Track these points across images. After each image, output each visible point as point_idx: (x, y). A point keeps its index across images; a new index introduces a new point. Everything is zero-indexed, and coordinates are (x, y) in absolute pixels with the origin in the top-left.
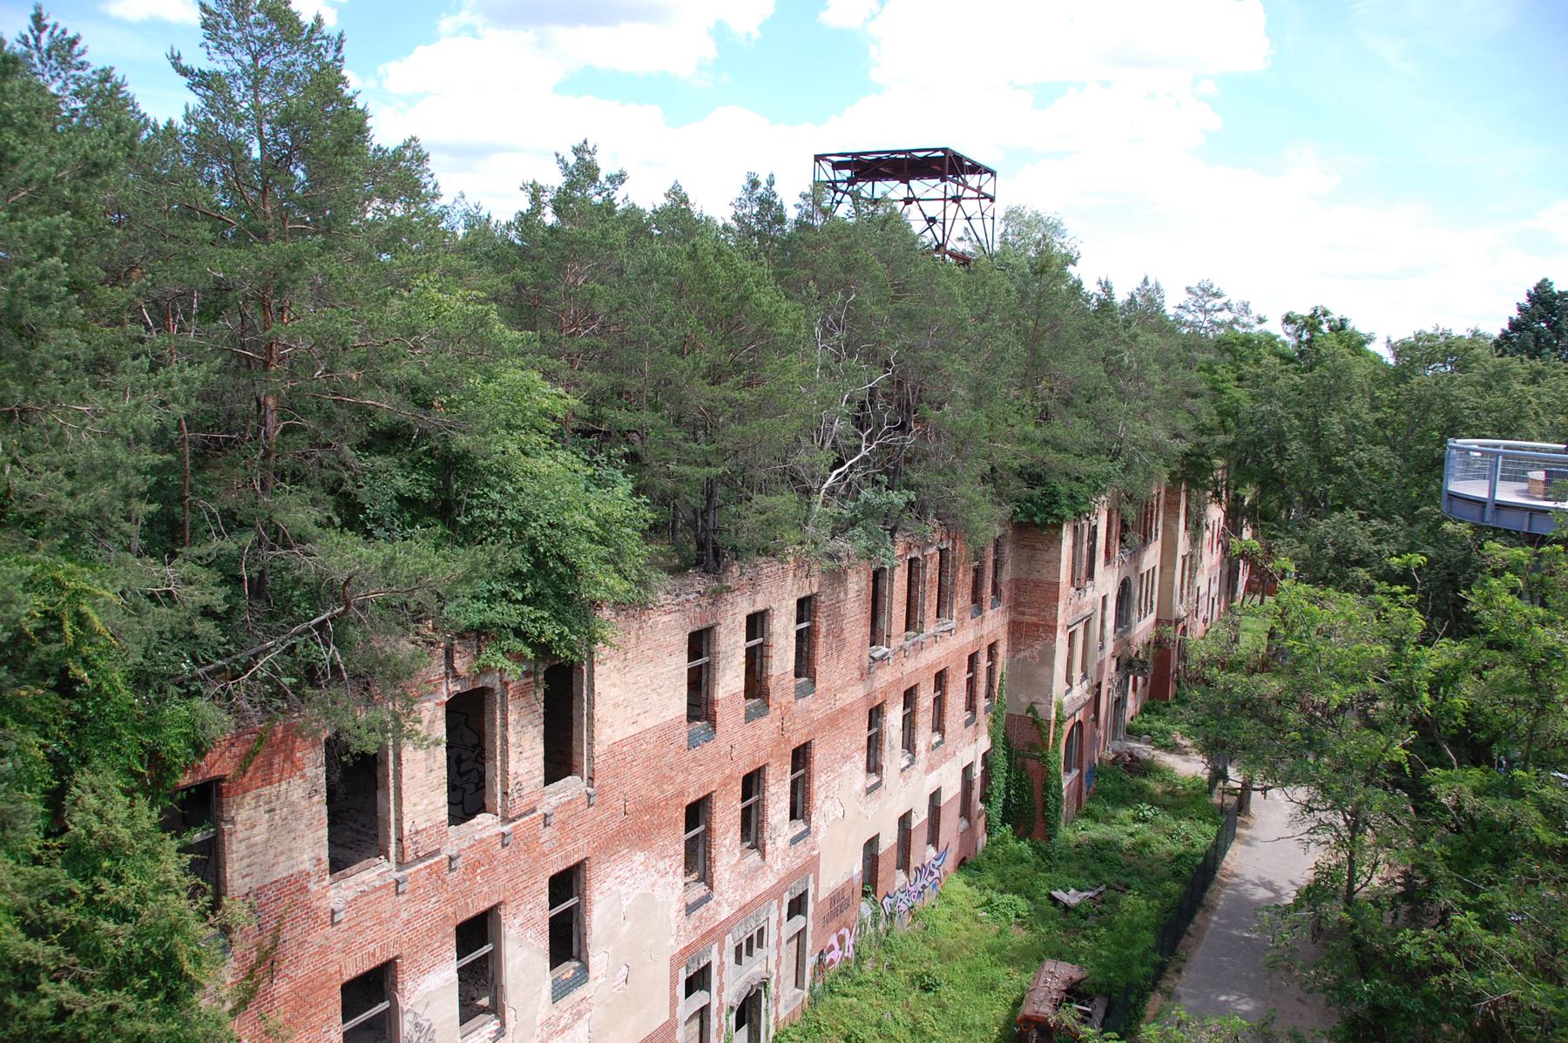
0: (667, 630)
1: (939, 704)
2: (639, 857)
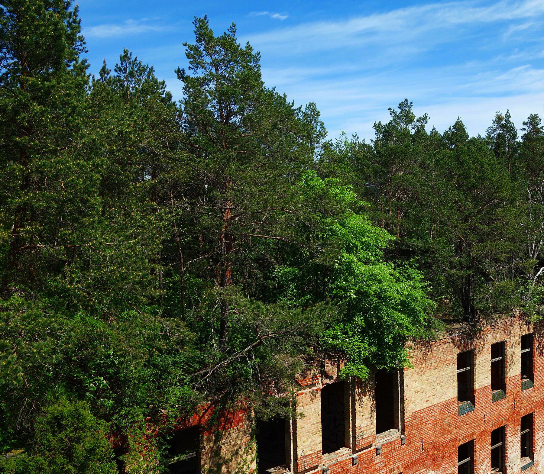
0: (446, 353)
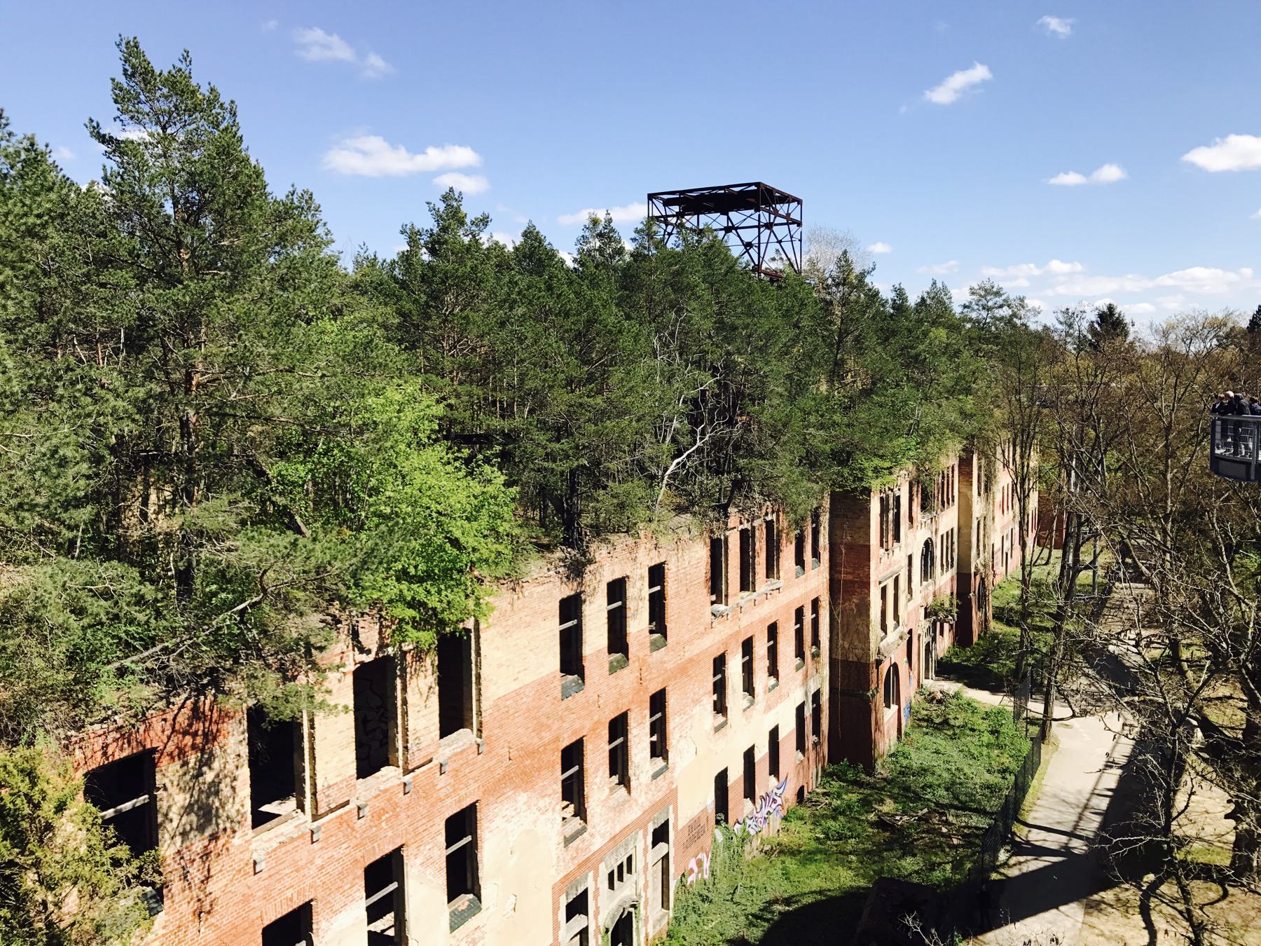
1: (773, 653)
2: (523, 797)
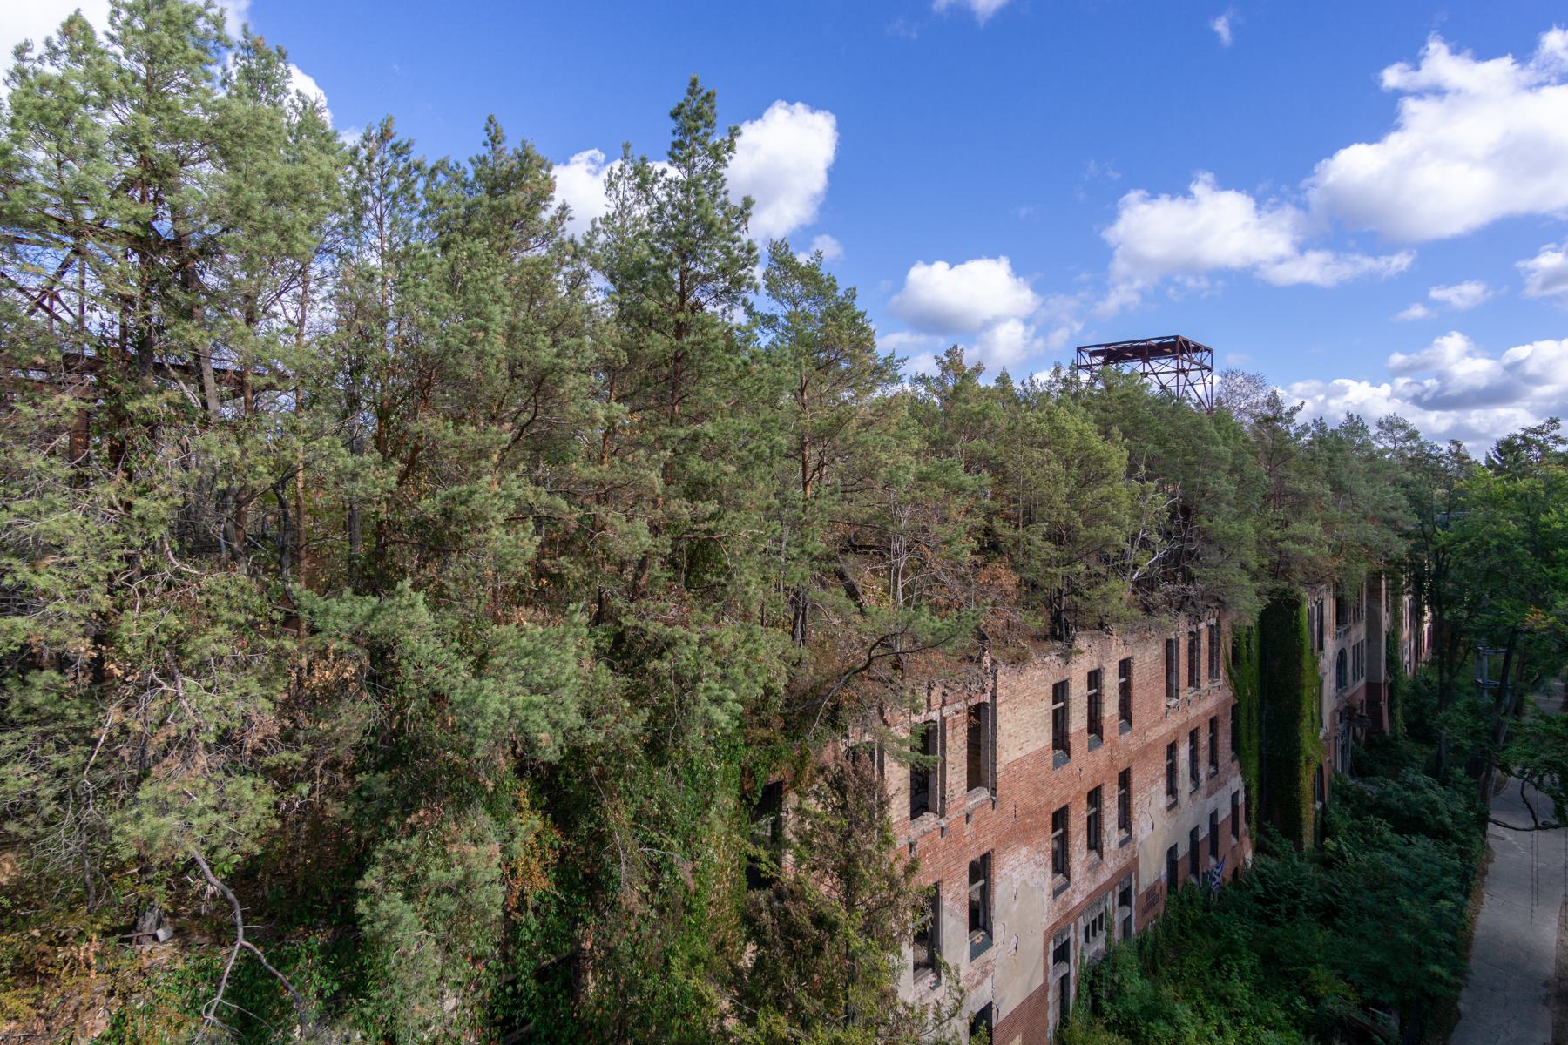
2: (1024, 851)
